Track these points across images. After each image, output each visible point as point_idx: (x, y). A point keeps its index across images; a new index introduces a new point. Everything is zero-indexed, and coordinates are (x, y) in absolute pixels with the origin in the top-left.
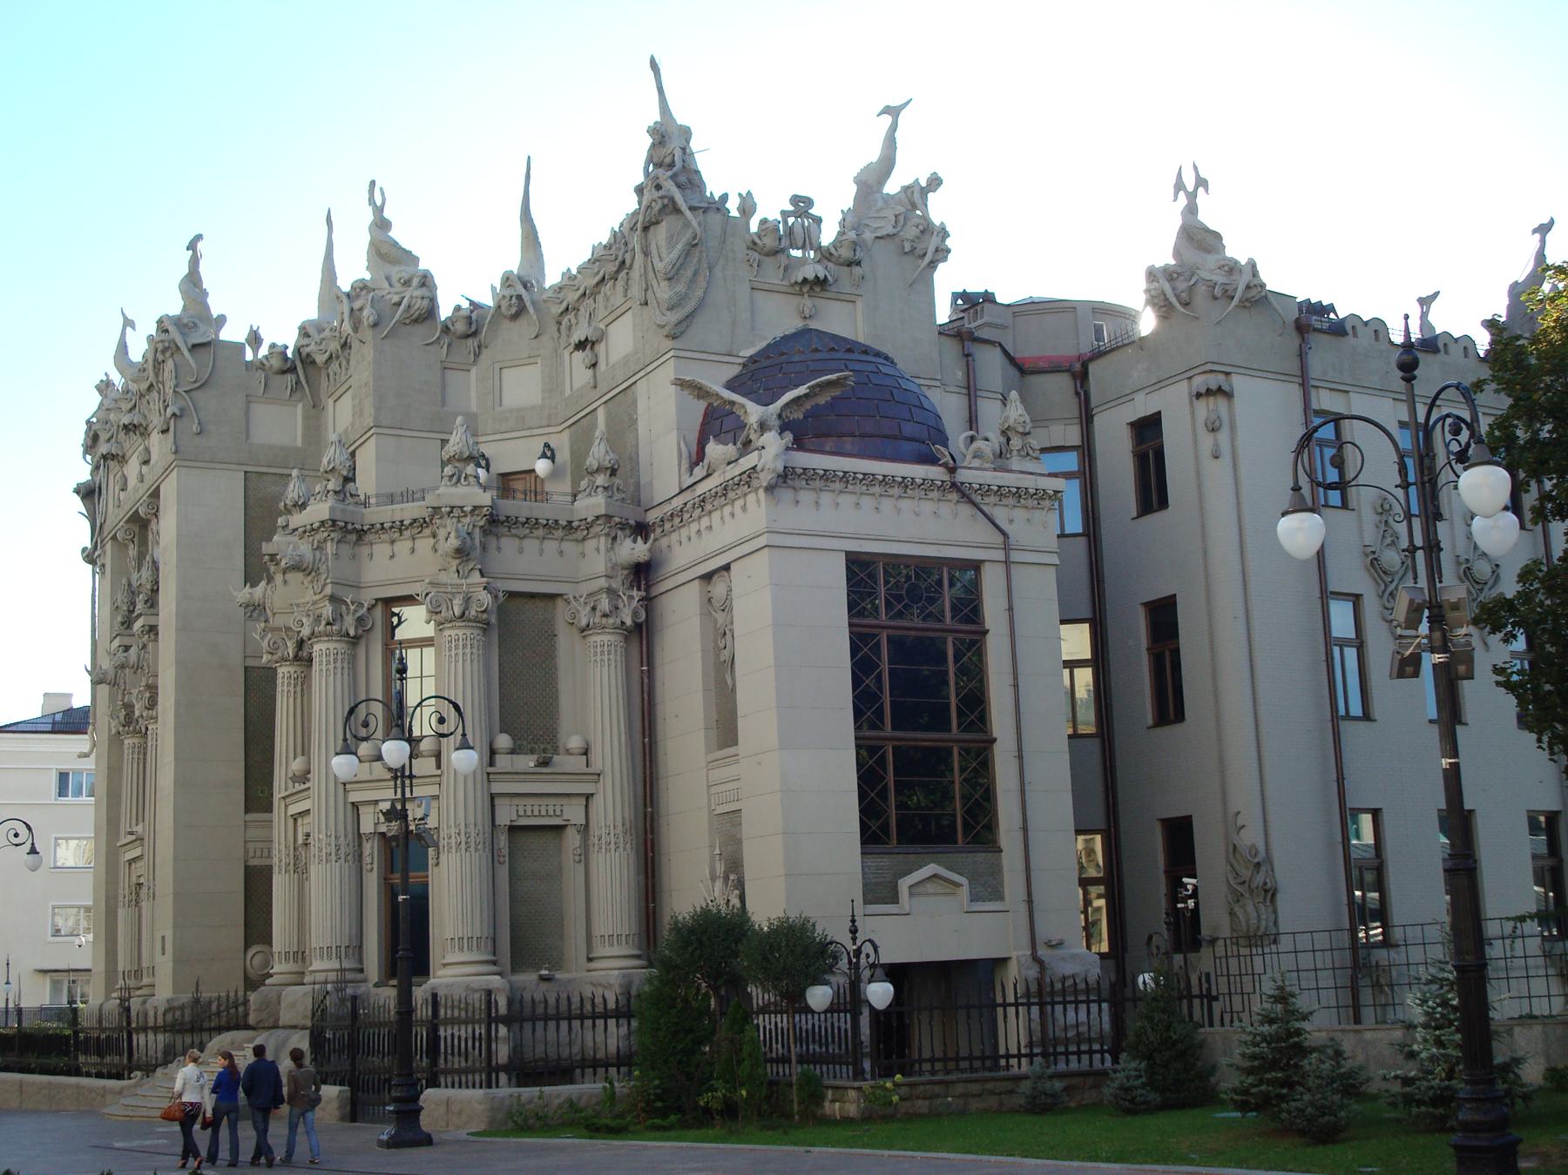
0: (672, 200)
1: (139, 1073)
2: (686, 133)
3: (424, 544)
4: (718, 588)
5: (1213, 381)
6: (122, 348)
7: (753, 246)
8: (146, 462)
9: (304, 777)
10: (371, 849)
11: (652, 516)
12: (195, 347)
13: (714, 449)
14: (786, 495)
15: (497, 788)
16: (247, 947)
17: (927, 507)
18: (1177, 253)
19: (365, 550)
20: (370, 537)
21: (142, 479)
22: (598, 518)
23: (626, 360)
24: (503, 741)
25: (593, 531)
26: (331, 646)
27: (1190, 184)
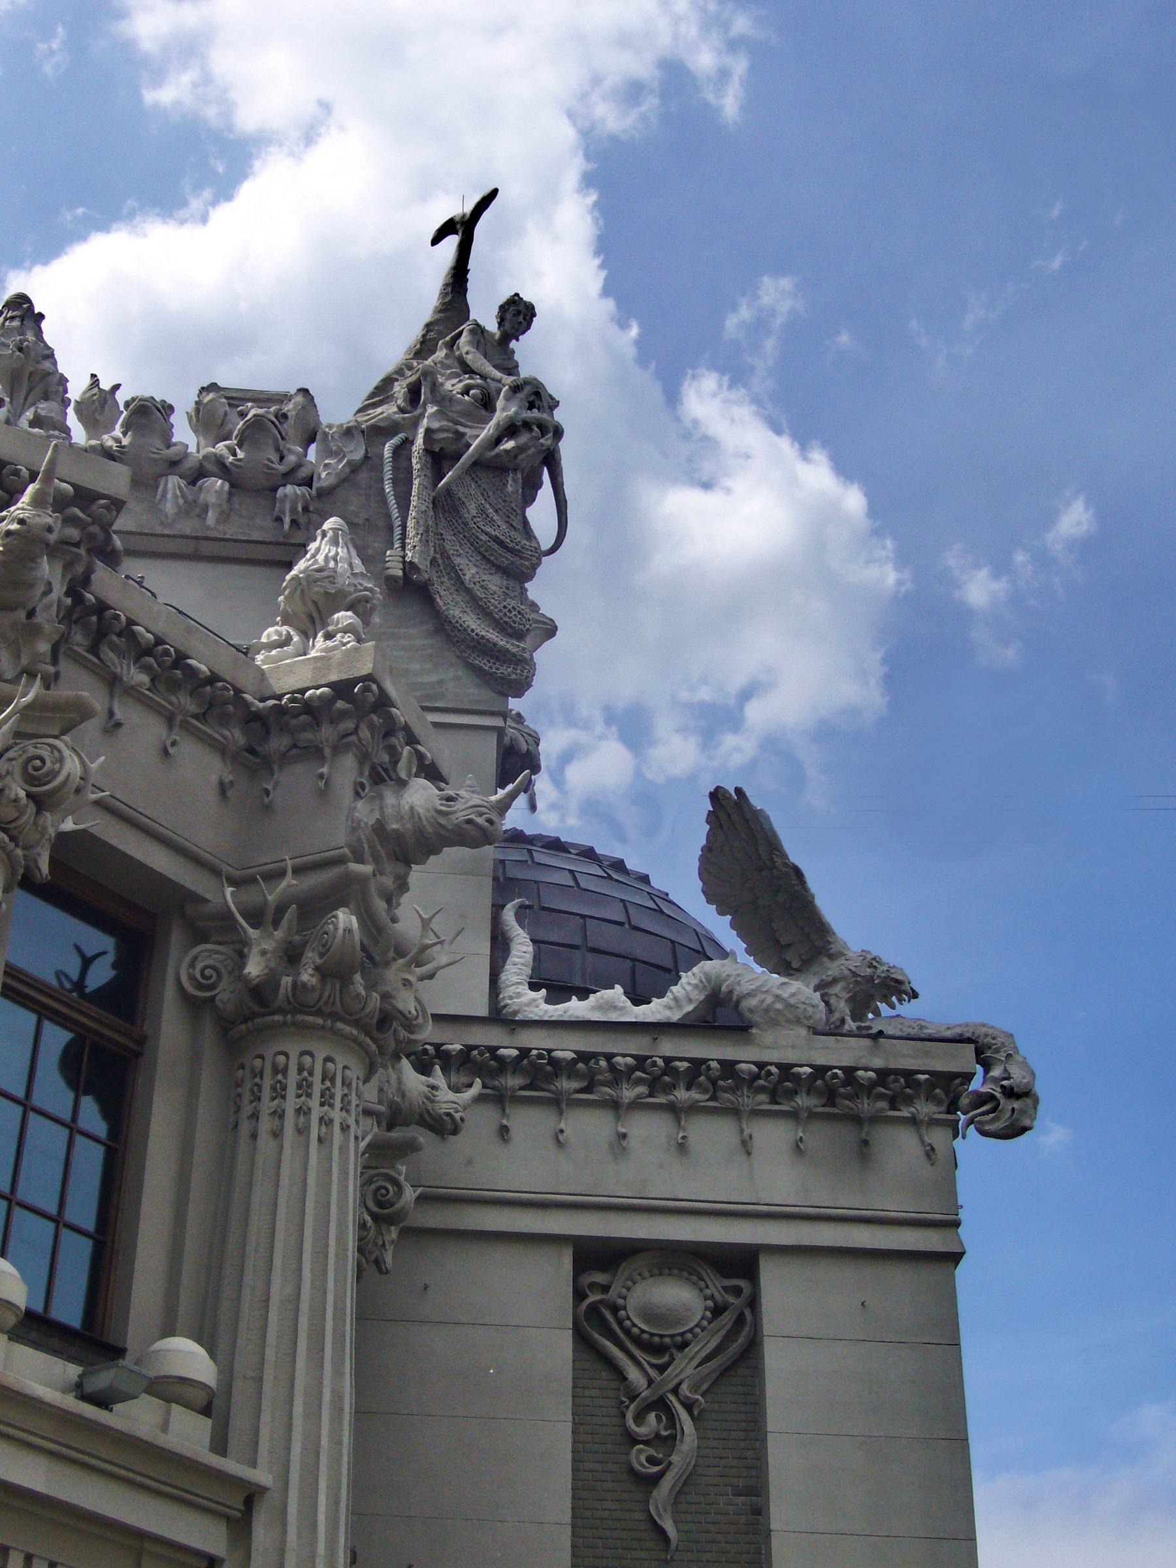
4: (677, 1297)
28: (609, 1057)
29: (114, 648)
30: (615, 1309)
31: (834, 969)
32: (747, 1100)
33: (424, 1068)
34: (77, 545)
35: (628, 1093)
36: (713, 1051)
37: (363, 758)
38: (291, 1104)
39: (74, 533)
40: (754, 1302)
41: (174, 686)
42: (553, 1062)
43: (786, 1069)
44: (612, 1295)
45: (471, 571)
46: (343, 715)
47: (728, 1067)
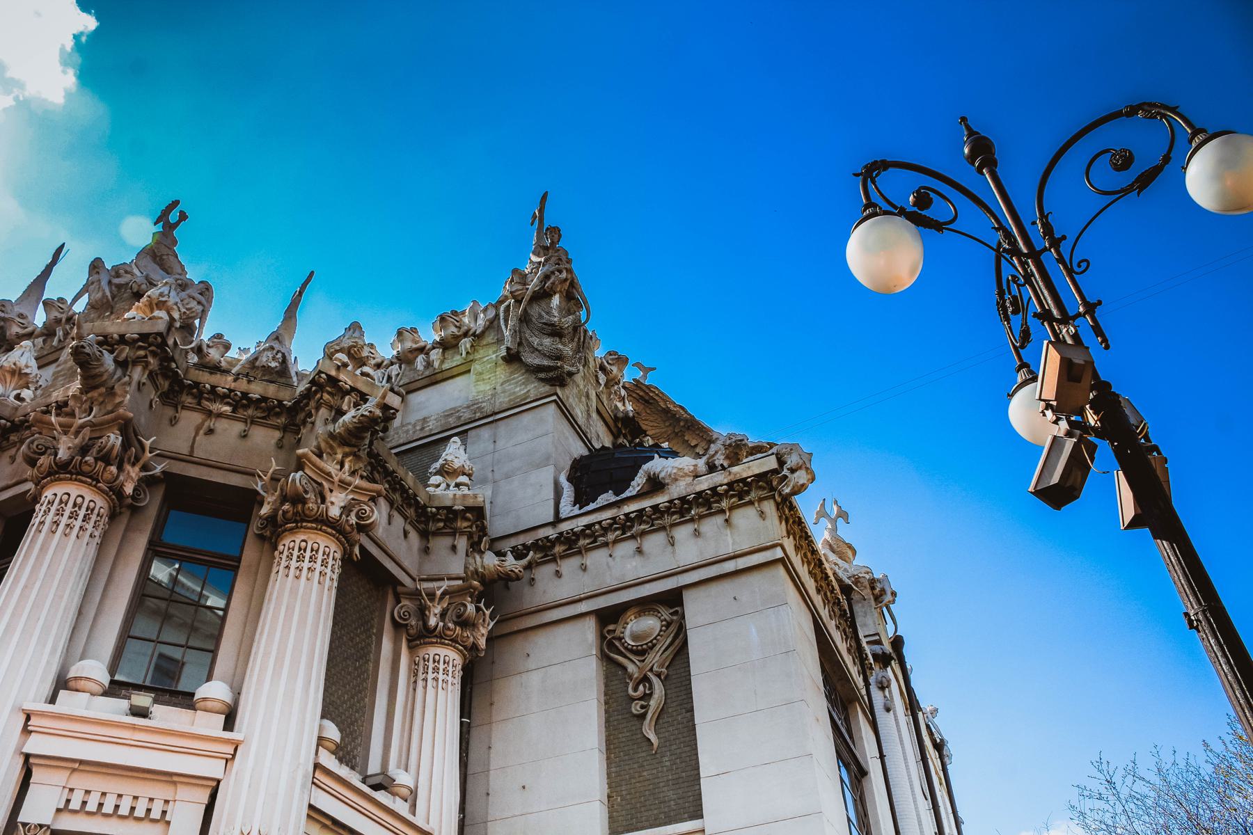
3: (264, 437)
7: (602, 368)
19: (169, 412)
22: (469, 509)
26: (89, 494)
28: (599, 523)
29: (208, 400)
30: (620, 639)
32: (667, 520)
34: (146, 356)
35: (611, 537)
36: (646, 504)
37: (331, 408)
38: (284, 563)
39: (142, 353)
40: (683, 617)
41: (246, 407)
42: (574, 534)
43: (683, 499)
44: (618, 633)
45: (535, 341)
46: (316, 392)
47: (655, 508)
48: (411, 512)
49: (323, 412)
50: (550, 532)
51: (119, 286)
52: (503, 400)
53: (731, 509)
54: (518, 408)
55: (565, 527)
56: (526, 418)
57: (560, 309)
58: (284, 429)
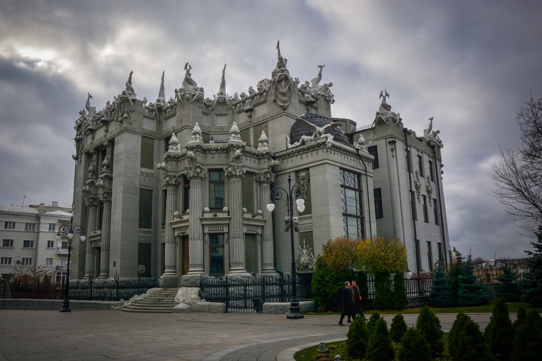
0: (287, 76)
1: (123, 300)
2: (286, 60)
3: (223, 156)
4: (303, 174)
5: (391, 139)
6: (88, 102)
7: (300, 91)
8: (107, 131)
9: (179, 216)
10: (207, 237)
11: (277, 155)
12: (133, 100)
13: (304, 137)
14: (329, 150)
15: (245, 222)
16: (139, 265)
17: (352, 158)
18: (380, 109)
20: (207, 152)
21: (105, 136)
23: (264, 115)
24: (245, 209)
25: (265, 156)
27: (384, 94)
31: (317, 131)
32: (305, 151)
33: (275, 160)
35: (296, 154)
36: (302, 147)
45: (279, 96)
48: (255, 156)
49: (232, 152)
50: (285, 153)
51: (183, 95)
52: (274, 113)
53: (318, 149)
54: (277, 116)
55: (287, 151)
56: (279, 118)
57: (284, 85)
58: (226, 153)
